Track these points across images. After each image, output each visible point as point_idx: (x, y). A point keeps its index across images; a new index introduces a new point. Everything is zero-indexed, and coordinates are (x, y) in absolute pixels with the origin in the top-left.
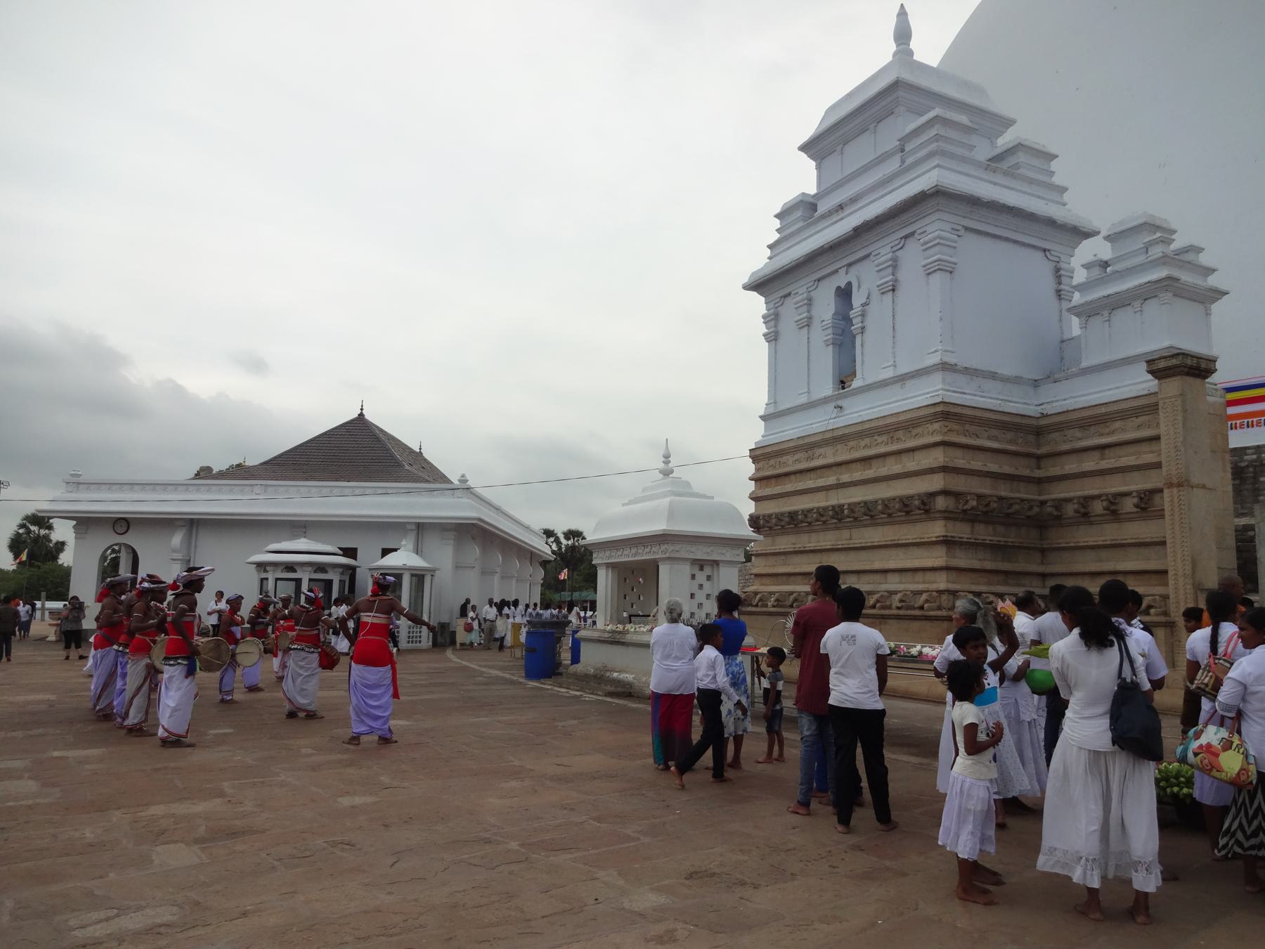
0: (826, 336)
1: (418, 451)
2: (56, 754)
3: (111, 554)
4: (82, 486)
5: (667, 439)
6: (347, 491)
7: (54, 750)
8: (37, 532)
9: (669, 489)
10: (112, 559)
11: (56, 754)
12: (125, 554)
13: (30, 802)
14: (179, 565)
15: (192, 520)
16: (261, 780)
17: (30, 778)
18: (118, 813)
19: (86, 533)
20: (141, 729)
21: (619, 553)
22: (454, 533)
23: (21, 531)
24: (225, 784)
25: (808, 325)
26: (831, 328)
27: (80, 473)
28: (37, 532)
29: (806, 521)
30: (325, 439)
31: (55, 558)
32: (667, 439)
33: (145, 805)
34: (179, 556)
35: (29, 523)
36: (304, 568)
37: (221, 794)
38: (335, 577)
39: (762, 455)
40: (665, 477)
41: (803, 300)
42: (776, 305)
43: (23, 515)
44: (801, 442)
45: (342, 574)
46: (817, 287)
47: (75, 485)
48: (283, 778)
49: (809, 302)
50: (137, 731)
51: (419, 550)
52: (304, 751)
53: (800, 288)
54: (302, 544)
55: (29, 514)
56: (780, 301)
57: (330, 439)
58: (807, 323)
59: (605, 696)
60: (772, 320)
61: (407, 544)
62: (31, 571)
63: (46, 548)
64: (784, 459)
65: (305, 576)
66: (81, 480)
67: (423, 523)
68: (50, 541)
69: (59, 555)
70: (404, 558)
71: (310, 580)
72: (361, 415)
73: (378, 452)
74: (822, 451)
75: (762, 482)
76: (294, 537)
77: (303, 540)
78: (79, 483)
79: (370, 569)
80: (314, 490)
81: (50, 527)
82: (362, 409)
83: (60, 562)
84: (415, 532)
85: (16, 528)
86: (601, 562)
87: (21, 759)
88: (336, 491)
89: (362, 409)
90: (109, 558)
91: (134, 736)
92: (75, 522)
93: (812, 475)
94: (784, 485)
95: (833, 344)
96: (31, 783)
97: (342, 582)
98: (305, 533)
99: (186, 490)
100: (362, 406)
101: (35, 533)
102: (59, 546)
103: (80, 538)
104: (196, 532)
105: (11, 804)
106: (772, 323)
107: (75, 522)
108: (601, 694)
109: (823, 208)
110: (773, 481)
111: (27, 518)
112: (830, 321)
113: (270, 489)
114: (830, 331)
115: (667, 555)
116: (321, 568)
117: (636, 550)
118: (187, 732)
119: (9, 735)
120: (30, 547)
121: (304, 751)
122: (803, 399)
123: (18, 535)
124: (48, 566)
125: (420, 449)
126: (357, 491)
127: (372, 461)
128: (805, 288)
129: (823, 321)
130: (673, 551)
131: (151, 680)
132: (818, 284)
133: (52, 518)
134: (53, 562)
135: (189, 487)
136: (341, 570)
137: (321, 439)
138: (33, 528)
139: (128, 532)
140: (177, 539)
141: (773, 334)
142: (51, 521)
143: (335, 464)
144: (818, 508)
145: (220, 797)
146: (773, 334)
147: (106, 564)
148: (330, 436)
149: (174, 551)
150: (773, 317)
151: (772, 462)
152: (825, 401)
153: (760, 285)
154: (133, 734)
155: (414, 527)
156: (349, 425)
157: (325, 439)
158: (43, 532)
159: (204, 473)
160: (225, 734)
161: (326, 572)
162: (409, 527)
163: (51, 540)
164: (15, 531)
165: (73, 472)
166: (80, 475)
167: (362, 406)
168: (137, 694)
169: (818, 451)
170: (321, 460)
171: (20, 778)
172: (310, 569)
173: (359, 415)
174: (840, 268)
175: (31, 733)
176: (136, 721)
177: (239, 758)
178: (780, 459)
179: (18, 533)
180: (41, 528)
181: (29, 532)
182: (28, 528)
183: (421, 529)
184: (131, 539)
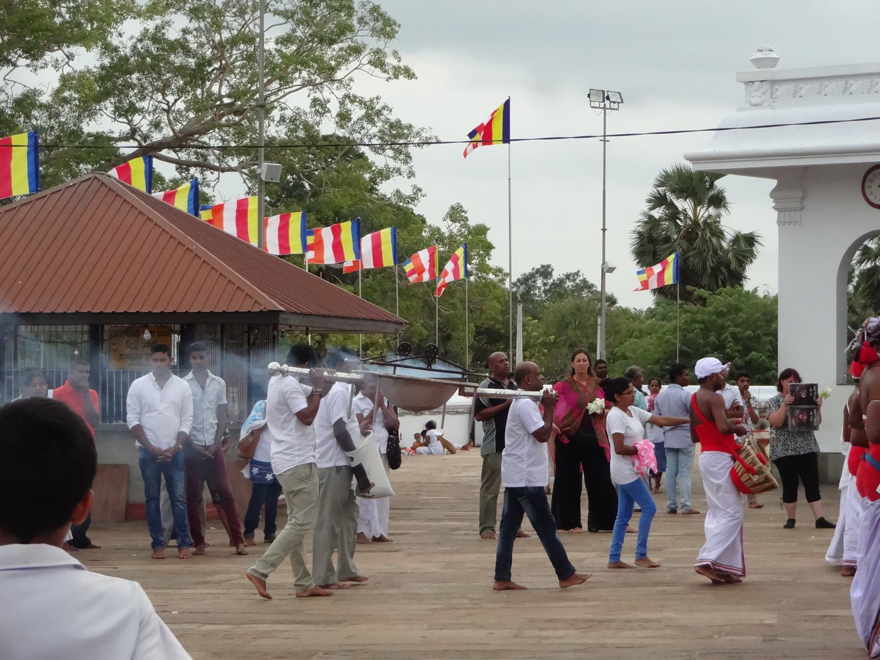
3: (860, 262)
4: (782, 89)
8: (690, 214)
10: (863, 274)
19: (802, 208)
23: (657, 213)
27: (774, 55)
28: (690, 213)
31: (737, 278)
35: (673, 191)
43: (655, 174)
47: (766, 87)
55: (670, 170)
62: (687, 312)
63: (715, 252)
66: (777, 72)
68: (720, 235)
69: (744, 269)
78: (774, 82)
81: (718, 201)
83: (748, 286)
85: (645, 207)
90: (857, 272)
92: (773, 183)
101: (686, 215)
102: (743, 244)
107: (773, 183)
111: (666, 180)
120: (680, 251)
123: (652, 223)
124: (720, 299)
133: (718, 175)
134: (733, 286)
138: (684, 204)
142: (719, 183)
147: (851, 288)
158: (704, 212)
163: (722, 233)
164: (645, 214)
165: (759, 55)
166: (776, 60)
179: (651, 217)
180: (698, 202)
181: (674, 214)
182: (671, 205)
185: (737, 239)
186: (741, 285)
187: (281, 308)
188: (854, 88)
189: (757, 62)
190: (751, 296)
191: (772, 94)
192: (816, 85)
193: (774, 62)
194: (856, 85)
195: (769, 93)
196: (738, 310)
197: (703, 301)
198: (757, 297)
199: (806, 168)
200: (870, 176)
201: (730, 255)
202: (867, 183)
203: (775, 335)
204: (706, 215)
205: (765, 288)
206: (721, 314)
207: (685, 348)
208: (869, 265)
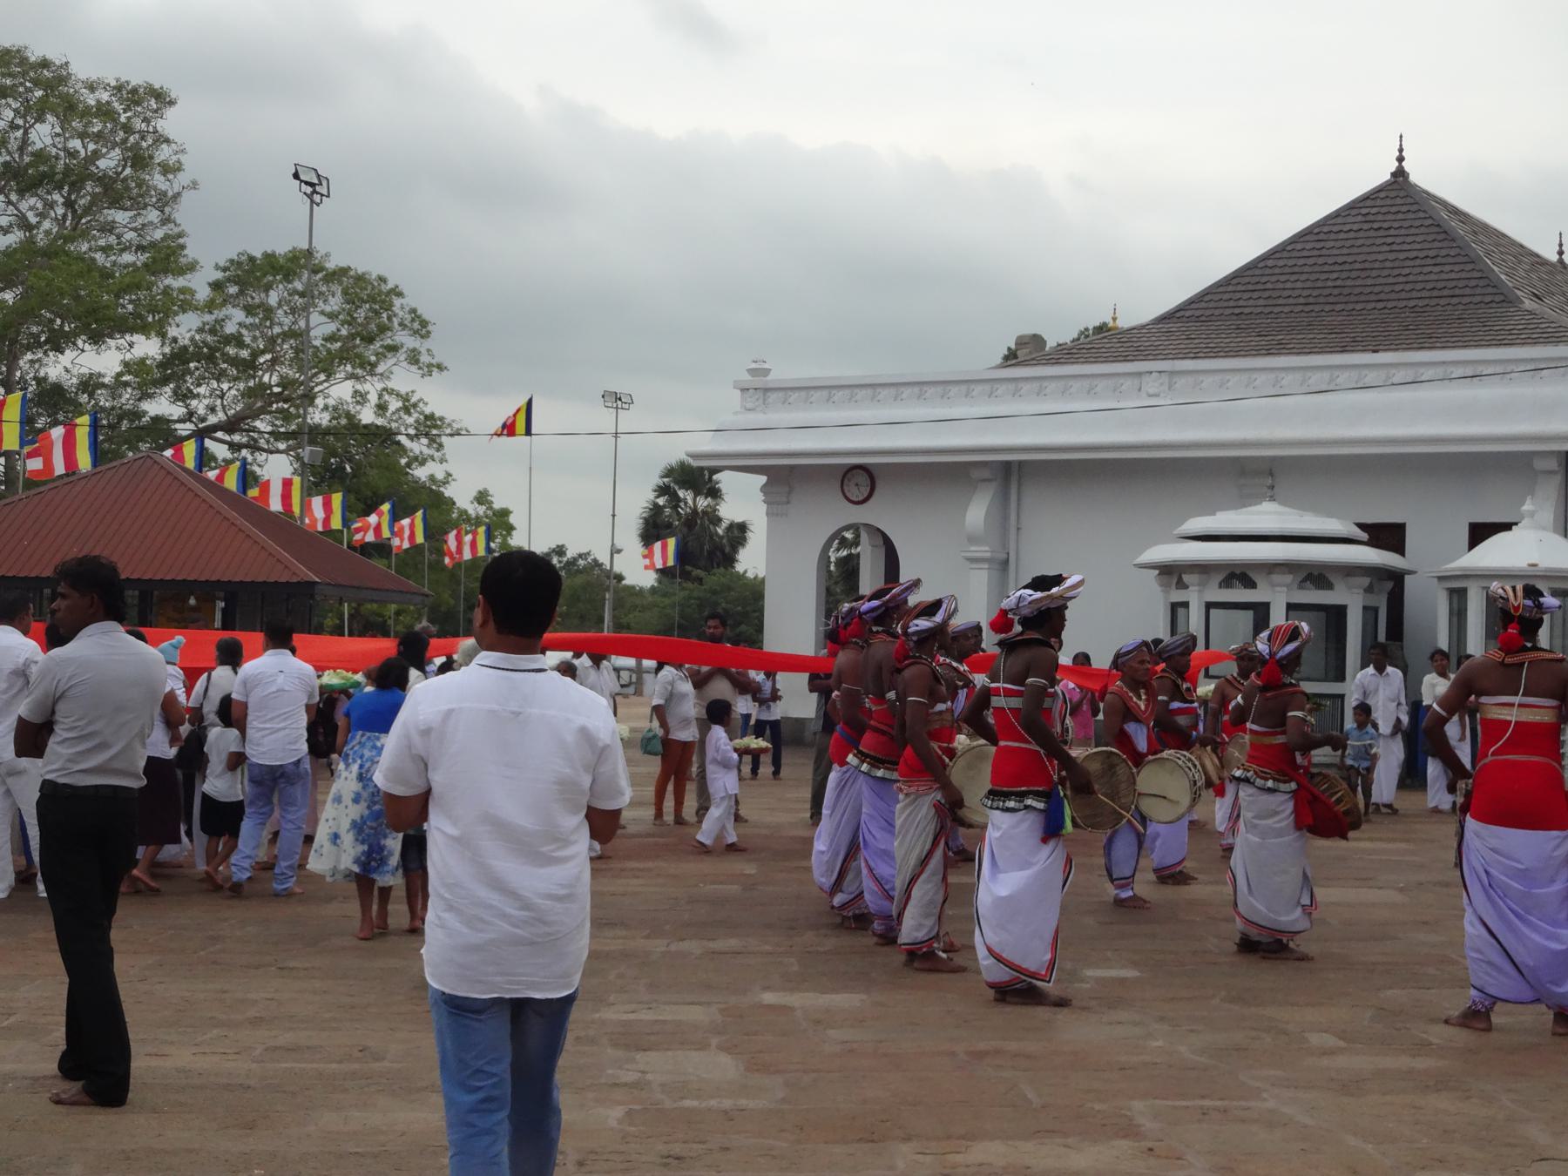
1: (1554, 258)
2: (769, 998)
3: (838, 550)
4: (773, 397)
6: (1371, 377)
7: (766, 988)
8: (690, 502)
11: (769, 998)
13: (727, 1103)
16: (1219, 1103)
17: (720, 1048)
18: (905, 1148)
19: (788, 502)
20: (931, 955)
23: (661, 501)
24: (1138, 1105)
28: (690, 502)
30: (1309, 246)
31: (730, 560)
33: (963, 1137)
34: (983, 551)
35: (676, 482)
36: (1276, 578)
37: (1129, 1130)
38: (1351, 598)
45: (1369, 590)
47: (759, 394)
48: (1271, 1104)
50: (922, 958)
52: (1315, 1039)
54: (1266, 516)
61: (1539, 509)
63: (711, 537)
65: (1277, 597)
72: (1400, 173)
73: (1447, 268)
76: (1245, 499)
77: (1267, 506)
78: (766, 390)
79: (1441, 578)
81: (715, 493)
82: (1400, 159)
85: (651, 495)
87: (700, 1004)
88: (1343, 378)
89: (1400, 159)
91: (917, 969)
92: (763, 479)
96: (724, 1059)
97: (1370, 612)
98: (1272, 487)
100: (1401, 150)
101: (686, 503)
102: (736, 532)
104: (1019, 494)
105: (688, 1103)
107: (763, 479)
111: (669, 472)
113: (1181, 382)
116: (1317, 575)
119: (673, 947)
120: (680, 535)
121: (1315, 1039)
123: (656, 510)
124: (715, 578)
125: (1561, 253)
131: (946, 843)
134: (726, 568)
136: (1366, 581)
137: (1299, 246)
138: (685, 494)
140: (977, 511)
142: (715, 477)
143: (1338, 307)
145: (1125, 1137)
148: (1322, 236)
149: (973, 539)
154: (916, 965)
155: (1553, 464)
156: (1369, 203)
157: (1309, 246)
158: (703, 503)
160: (1122, 981)
162: (1539, 464)
163: (720, 520)
165: (754, 366)
167: (1401, 150)
168: (921, 872)
170: (1302, 300)
171: (703, 1046)
172: (1288, 578)
173: (1394, 175)
175: (713, 945)
176: (921, 935)
177: (1160, 1043)
179: (656, 505)
180: (697, 493)
181: (675, 501)
184: (880, 513)
185: (732, 526)
186: (734, 567)
188: (835, 398)
189: (752, 372)
190: (741, 577)
191: (764, 400)
192: (803, 393)
193: (767, 372)
194: (839, 394)
195: (761, 401)
196: (729, 589)
197: (700, 580)
198: (746, 578)
199: (792, 468)
200: (849, 475)
201: (725, 541)
202: (846, 481)
203: (761, 611)
204: (706, 503)
205: (754, 570)
206: (714, 593)
207: (683, 622)
208: (845, 553)
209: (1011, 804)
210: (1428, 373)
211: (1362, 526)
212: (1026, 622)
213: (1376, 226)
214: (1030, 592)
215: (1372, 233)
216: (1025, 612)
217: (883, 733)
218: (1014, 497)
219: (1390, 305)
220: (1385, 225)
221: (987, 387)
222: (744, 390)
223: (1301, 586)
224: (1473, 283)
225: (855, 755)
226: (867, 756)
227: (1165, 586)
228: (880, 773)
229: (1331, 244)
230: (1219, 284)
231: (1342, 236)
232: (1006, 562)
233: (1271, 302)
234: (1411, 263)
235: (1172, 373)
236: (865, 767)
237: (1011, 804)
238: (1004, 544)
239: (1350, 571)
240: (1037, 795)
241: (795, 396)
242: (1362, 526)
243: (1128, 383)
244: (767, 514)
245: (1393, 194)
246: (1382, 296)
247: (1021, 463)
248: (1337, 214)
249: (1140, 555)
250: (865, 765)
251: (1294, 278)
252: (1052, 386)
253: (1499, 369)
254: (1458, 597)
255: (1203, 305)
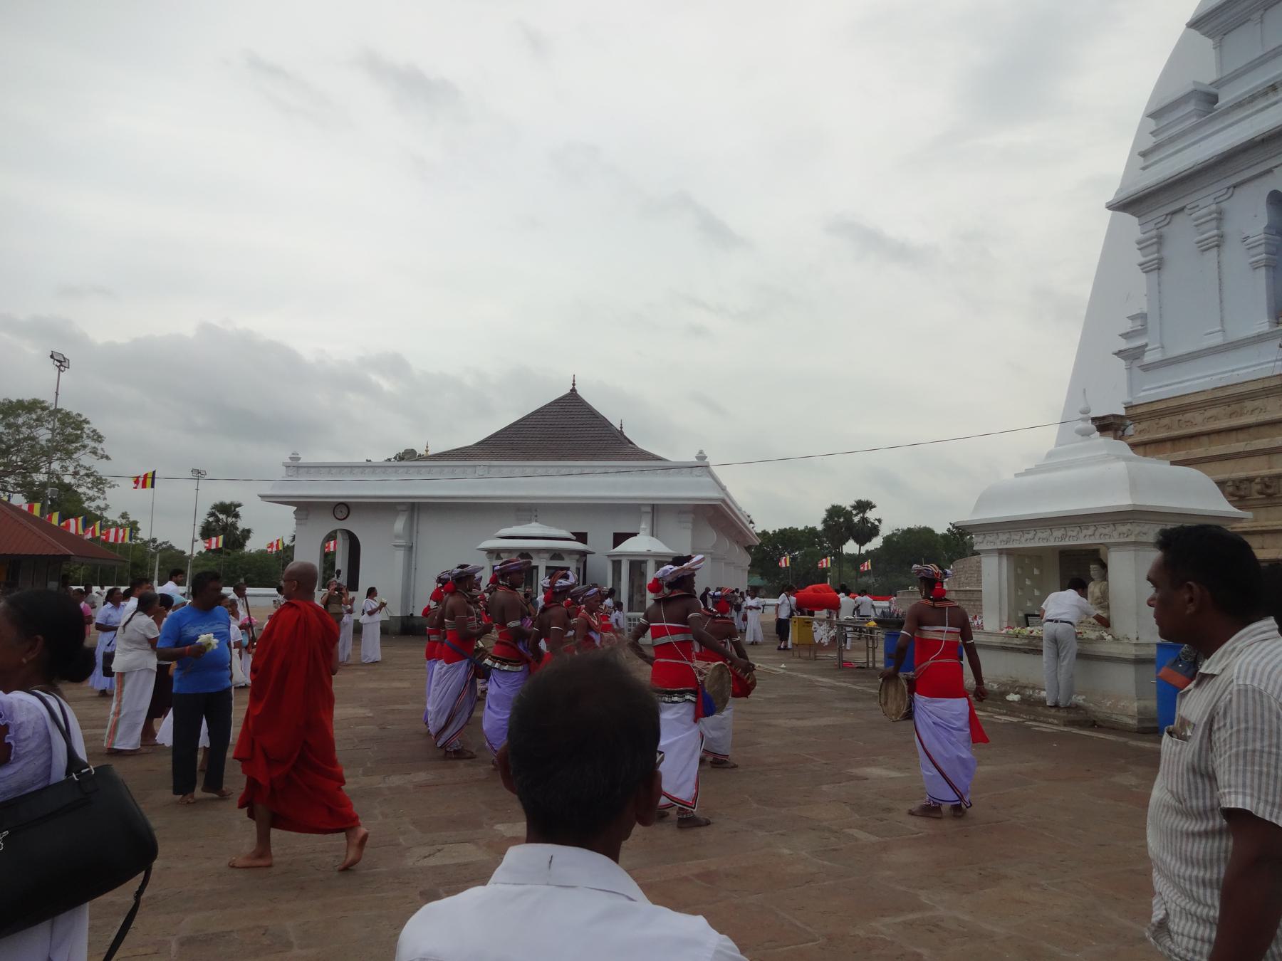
0: (1253, 256)
1: (620, 429)
4: (302, 470)
5: (1085, 390)
6: (551, 471)
9: (1103, 453)
12: (341, 541)
14: (403, 552)
15: (413, 504)
19: (307, 519)
21: (1030, 536)
22: (693, 516)
25: (1218, 246)
26: (1264, 246)
29: (1238, 494)
30: (539, 417)
32: (1085, 390)
34: (401, 542)
36: (541, 555)
38: (571, 563)
39: (1149, 413)
40: (1085, 438)
41: (1210, 214)
42: (1159, 225)
44: (1219, 394)
45: (578, 561)
46: (1232, 196)
47: (295, 469)
49: (1220, 216)
51: (655, 532)
53: (1204, 200)
54: (534, 528)
56: (1165, 219)
57: (543, 417)
58: (1219, 243)
59: (1065, 725)
60: (1154, 243)
61: (645, 526)
64: (1188, 416)
65: (541, 563)
67: (657, 505)
70: (641, 544)
71: (547, 568)
72: (573, 390)
73: (597, 429)
74: (1257, 403)
75: (1147, 447)
76: (519, 522)
77: (534, 524)
78: (298, 467)
79: (608, 556)
80: (517, 470)
82: (574, 385)
84: (650, 515)
86: (990, 547)
88: (540, 471)
89: (574, 385)
92: (295, 508)
93: (1241, 435)
94: (1190, 449)
95: (1265, 266)
97: (578, 569)
98: (536, 516)
99: (396, 472)
100: (574, 381)
103: (301, 524)
104: (418, 519)
106: (1155, 248)
107: (295, 508)
108: (1056, 721)
109: (1226, 98)
110: (1169, 445)
112: (1263, 236)
113: (493, 470)
114: (1262, 249)
115: (1132, 539)
116: (557, 554)
117: (1062, 531)
118: (695, 799)
122: (1217, 340)
125: (621, 428)
126: (564, 471)
127: (592, 439)
128: (1210, 200)
129: (1245, 239)
130: (1139, 534)
132: (1233, 192)
135: (409, 469)
136: (577, 557)
137: (535, 417)
139: (350, 516)
140: (399, 524)
141: (1156, 261)
143: (554, 442)
144: (1262, 478)
146: (1156, 261)
148: (544, 413)
149: (397, 537)
150: (1155, 240)
151: (1166, 421)
152: (1259, 339)
153: (1129, 204)
155: (649, 509)
156: (562, 401)
157: (539, 417)
159: (408, 455)
161: (561, 558)
162: (644, 509)
167: (574, 381)
169: (1249, 405)
170: (538, 439)
172: (547, 556)
173: (571, 390)
174: (1276, 167)
178: (1180, 417)
183: (657, 511)
184: (351, 525)
187: (72, 553)
209: (676, 699)
210: (611, 470)
211: (573, 534)
212: (670, 585)
213: (566, 410)
214: (671, 566)
215: (565, 413)
216: (669, 579)
217: (506, 644)
218: (416, 517)
219: (575, 442)
220: (570, 410)
221: (383, 469)
222: (287, 467)
223: (552, 558)
224: (608, 435)
225: (489, 659)
226: (497, 658)
227: (490, 558)
228: (506, 668)
229: (547, 417)
230: (502, 430)
231: (552, 413)
232: (412, 547)
233: (525, 439)
234: (582, 426)
235: (490, 466)
236: (497, 665)
237: (676, 699)
238: (411, 537)
239: (571, 552)
240: (691, 692)
241: (312, 470)
242: (573, 534)
243: (470, 470)
244: (296, 524)
245: (571, 398)
246: (571, 439)
247: (419, 503)
248: (550, 405)
249: (479, 545)
250: (497, 664)
251: (534, 429)
252: (423, 470)
253: (616, 470)
254: (617, 565)
255: (495, 439)
